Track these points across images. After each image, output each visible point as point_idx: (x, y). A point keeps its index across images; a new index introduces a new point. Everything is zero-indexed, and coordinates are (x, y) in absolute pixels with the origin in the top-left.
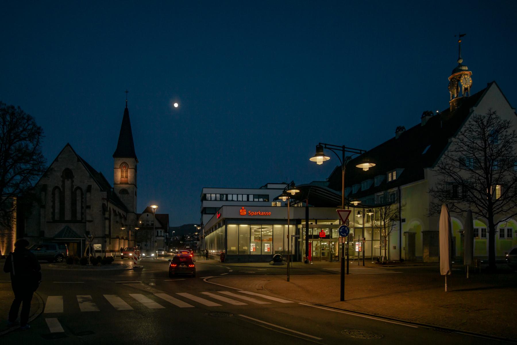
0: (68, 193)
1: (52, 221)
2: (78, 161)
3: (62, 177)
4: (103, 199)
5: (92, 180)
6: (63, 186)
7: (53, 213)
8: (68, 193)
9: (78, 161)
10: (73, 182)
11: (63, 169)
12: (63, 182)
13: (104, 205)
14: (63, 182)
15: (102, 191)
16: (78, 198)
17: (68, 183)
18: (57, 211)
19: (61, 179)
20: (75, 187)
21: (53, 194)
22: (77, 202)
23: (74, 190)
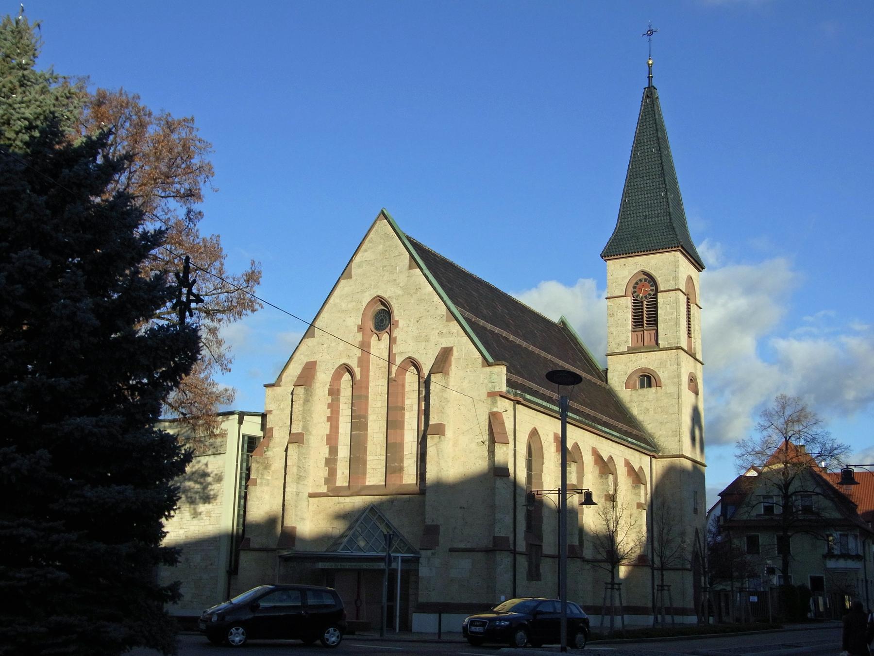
0: (377, 387)
1: (324, 489)
2: (410, 268)
3: (360, 329)
4: (492, 395)
5: (455, 327)
6: (364, 362)
7: (331, 462)
8: (377, 387)
9: (410, 268)
10: (392, 341)
11: (367, 298)
12: (364, 347)
13: (494, 419)
14: (364, 347)
15: (489, 365)
16: (407, 402)
17: (379, 347)
18: (343, 452)
19: (359, 337)
20: (399, 360)
21: (334, 392)
22: (407, 415)
23: (394, 369)
